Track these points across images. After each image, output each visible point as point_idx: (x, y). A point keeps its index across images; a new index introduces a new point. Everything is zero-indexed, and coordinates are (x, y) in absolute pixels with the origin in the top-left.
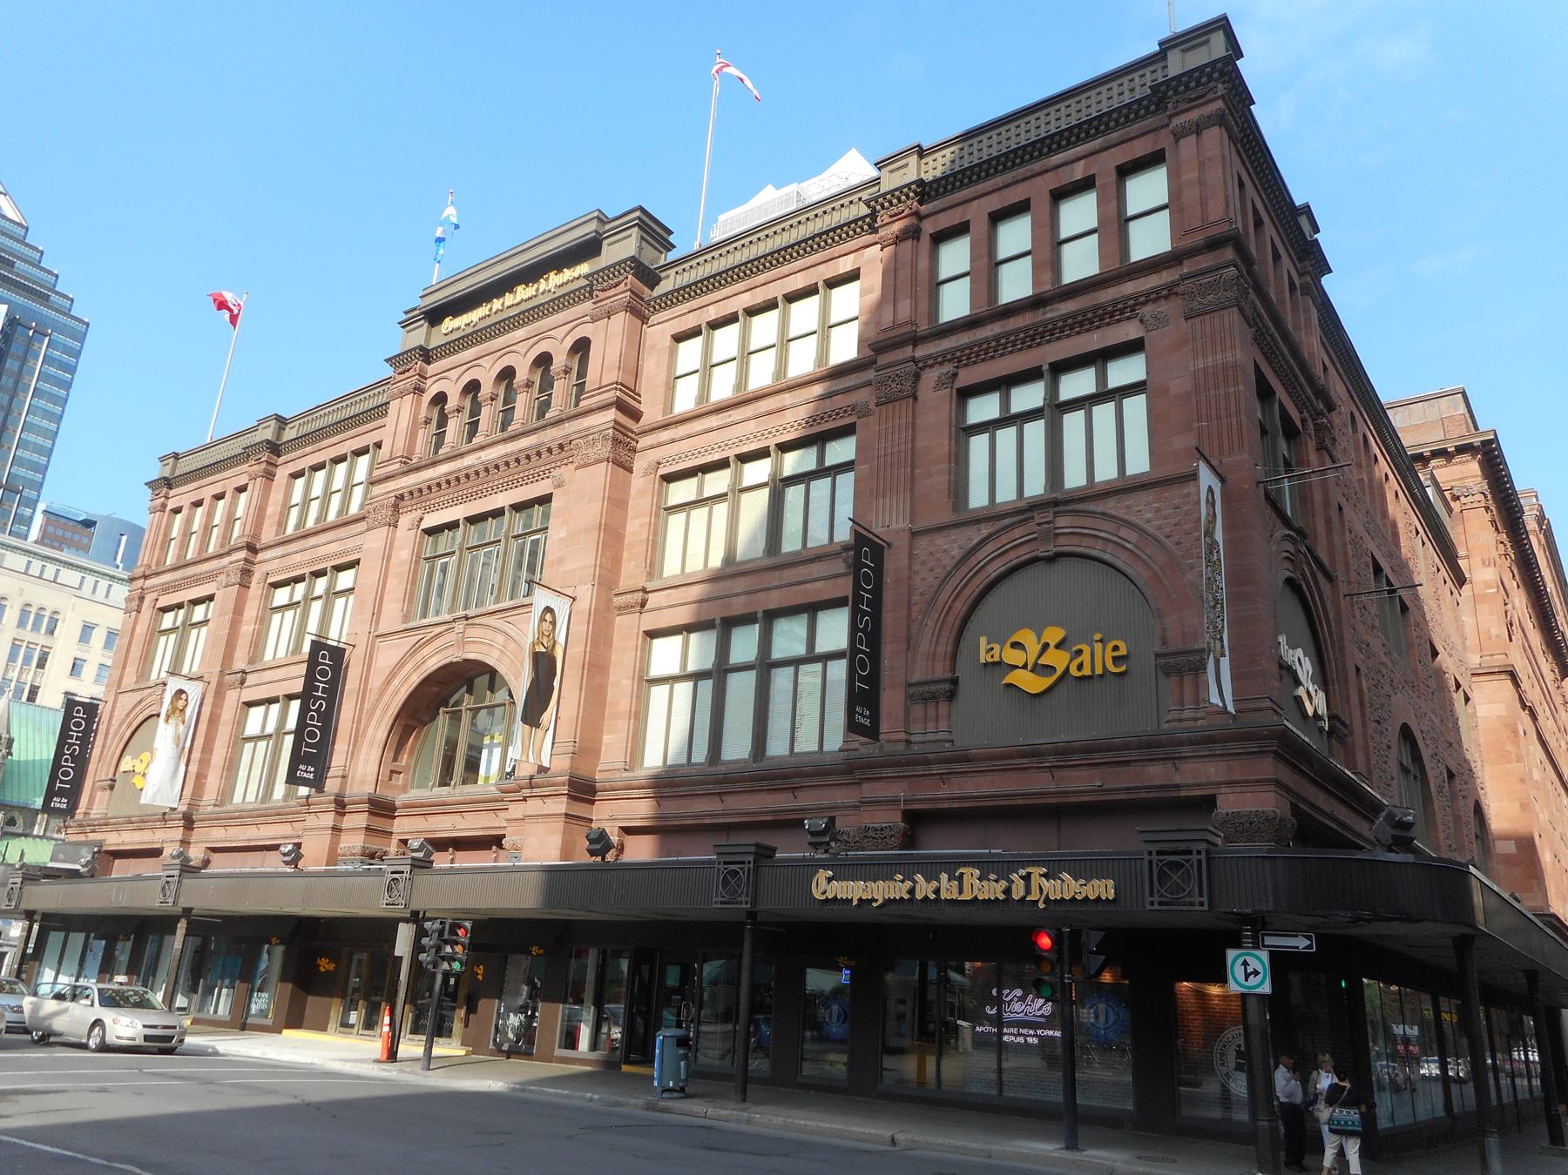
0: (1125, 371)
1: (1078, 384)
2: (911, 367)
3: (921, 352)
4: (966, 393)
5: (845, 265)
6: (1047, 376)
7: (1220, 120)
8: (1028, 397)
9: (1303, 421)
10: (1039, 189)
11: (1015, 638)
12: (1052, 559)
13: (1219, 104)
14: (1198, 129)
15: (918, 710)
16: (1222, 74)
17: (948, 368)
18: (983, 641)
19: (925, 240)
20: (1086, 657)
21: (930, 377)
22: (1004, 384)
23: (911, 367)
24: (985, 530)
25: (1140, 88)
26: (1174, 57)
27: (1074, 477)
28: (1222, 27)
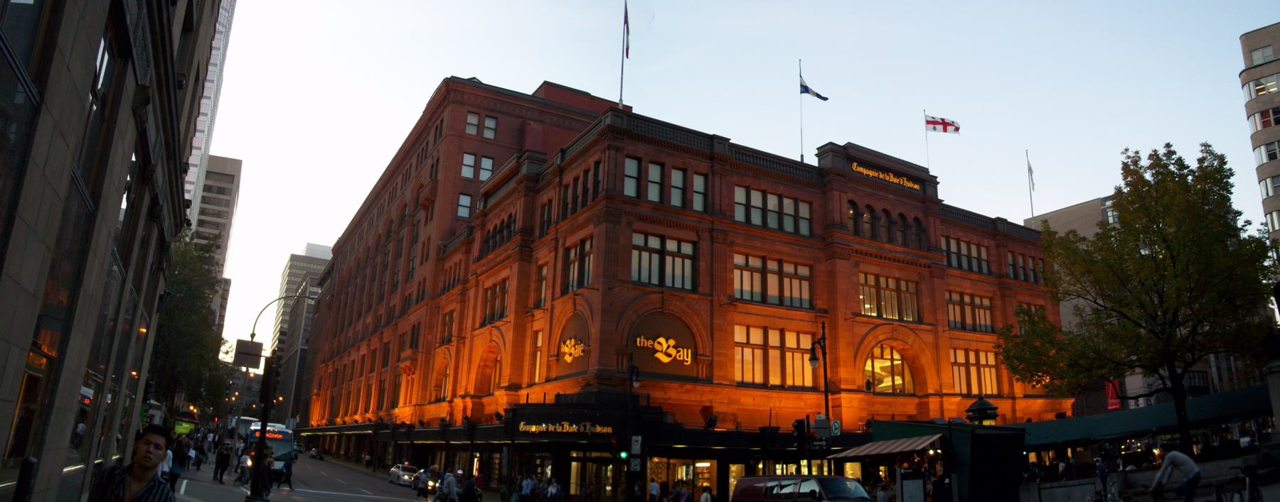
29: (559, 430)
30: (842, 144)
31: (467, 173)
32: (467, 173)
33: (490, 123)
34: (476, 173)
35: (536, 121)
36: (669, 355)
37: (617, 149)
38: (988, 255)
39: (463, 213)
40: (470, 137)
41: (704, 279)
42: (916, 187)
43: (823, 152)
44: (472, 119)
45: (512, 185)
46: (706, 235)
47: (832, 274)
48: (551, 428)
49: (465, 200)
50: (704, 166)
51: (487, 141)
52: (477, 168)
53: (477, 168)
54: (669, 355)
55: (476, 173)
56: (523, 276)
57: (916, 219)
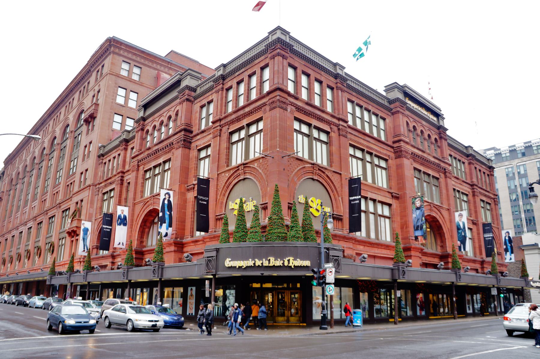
0: (261, 125)
1: (253, 129)
2: (219, 128)
3: (223, 122)
4: (231, 133)
5: (210, 99)
6: (246, 128)
7: (279, 54)
8: (243, 134)
9: (331, 128)
10: (245, 76)
11: (236, 202)
12: (244, 179)
13: (278, 50)
14: (273, 58)
15: (218, 222)
16: (278, 42)
17: (227, 127)
18: (230, 203)
19: (225, 91)
20: (248, 206)
21: (224, 129)
22: (239, 130)
23: (219, 128)
24: (232, 172)
25: (262, 47)
26: (270, 36)
27: (252, 157)
28: (279, 29)
29: (266, 263)
30: (401, 84)
31: (120, 100)
32: (120, 100)
33: (136, 70)
34: (126, 101)
35: (166, 73)
36: (318, 210)
37: (284, 57)
38: (465, 168)
39: (116, 127)
40: (123, 78)
41: (336, 158)
42: (435, 119)
43: (390, 88)
44: (125, 66)
45: (174, 94)
46: (335, 129)
47: (400, 167)
48: (258, 263)
49: (118, 118)
50: (332, 81)
51: (134, 82)
52: (127, 98)
53: (127, 98)
54: (318, 210)
55: (126, 101)
56: (186, 158)
57: (436, 139)
